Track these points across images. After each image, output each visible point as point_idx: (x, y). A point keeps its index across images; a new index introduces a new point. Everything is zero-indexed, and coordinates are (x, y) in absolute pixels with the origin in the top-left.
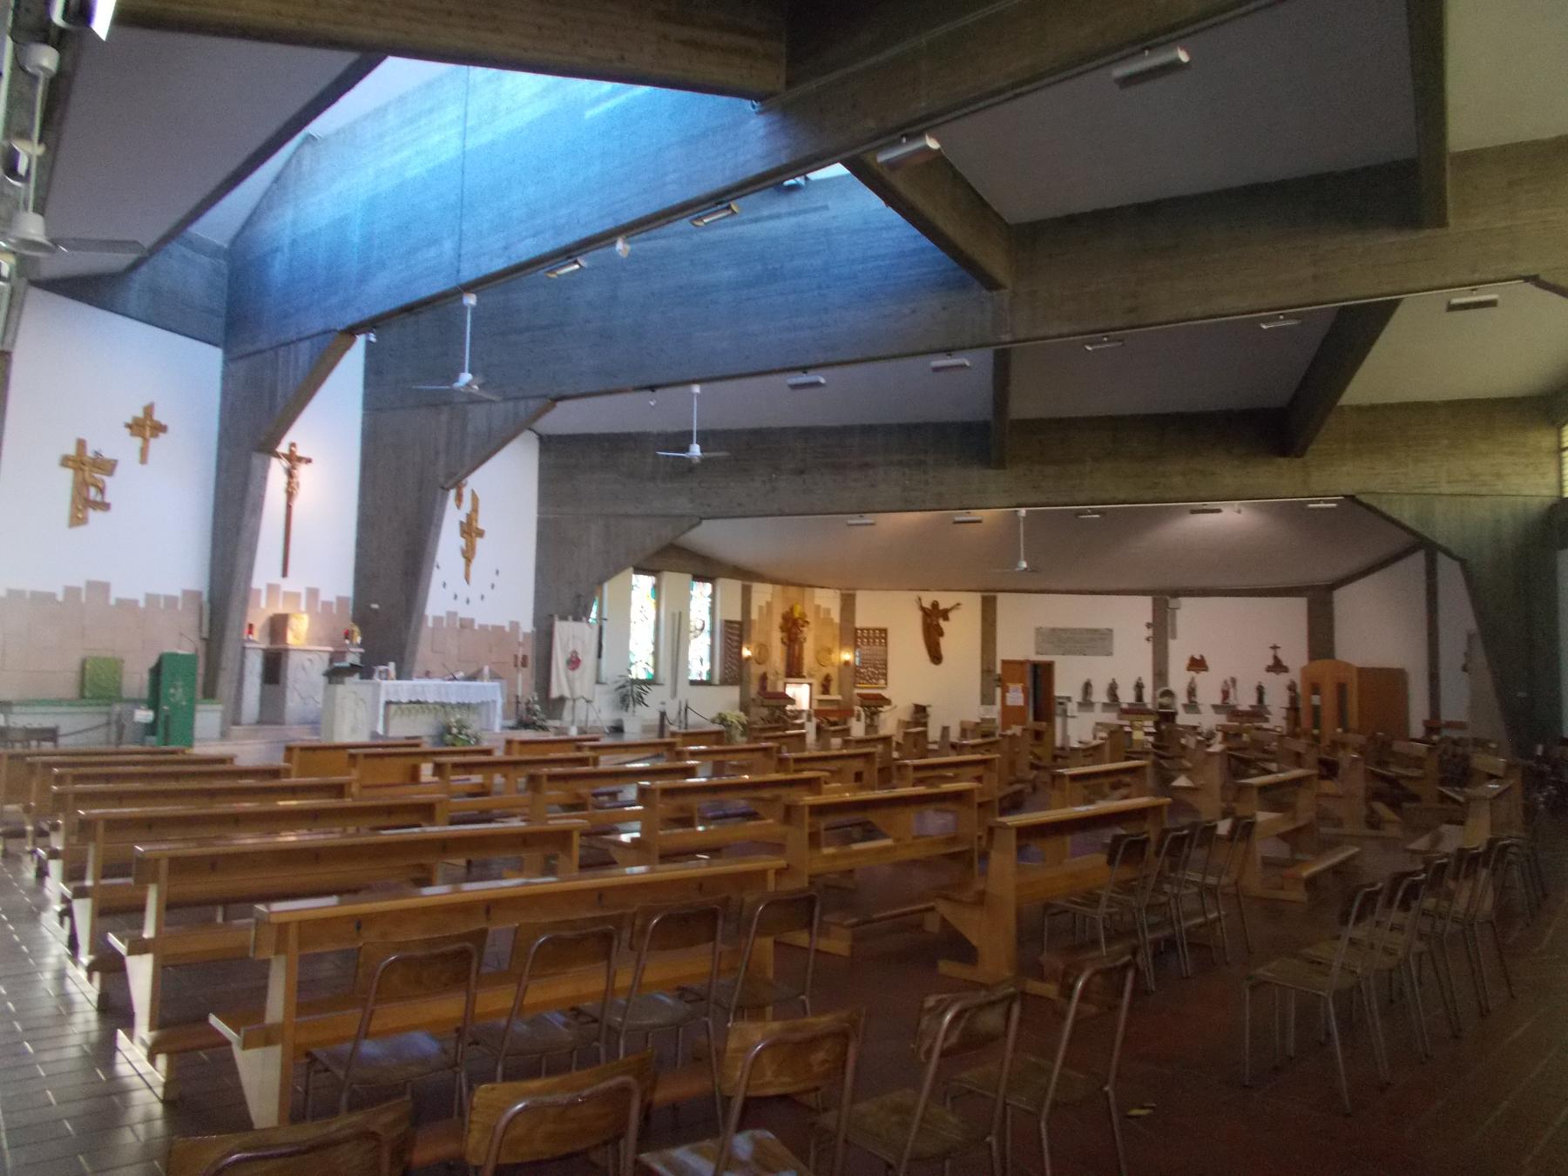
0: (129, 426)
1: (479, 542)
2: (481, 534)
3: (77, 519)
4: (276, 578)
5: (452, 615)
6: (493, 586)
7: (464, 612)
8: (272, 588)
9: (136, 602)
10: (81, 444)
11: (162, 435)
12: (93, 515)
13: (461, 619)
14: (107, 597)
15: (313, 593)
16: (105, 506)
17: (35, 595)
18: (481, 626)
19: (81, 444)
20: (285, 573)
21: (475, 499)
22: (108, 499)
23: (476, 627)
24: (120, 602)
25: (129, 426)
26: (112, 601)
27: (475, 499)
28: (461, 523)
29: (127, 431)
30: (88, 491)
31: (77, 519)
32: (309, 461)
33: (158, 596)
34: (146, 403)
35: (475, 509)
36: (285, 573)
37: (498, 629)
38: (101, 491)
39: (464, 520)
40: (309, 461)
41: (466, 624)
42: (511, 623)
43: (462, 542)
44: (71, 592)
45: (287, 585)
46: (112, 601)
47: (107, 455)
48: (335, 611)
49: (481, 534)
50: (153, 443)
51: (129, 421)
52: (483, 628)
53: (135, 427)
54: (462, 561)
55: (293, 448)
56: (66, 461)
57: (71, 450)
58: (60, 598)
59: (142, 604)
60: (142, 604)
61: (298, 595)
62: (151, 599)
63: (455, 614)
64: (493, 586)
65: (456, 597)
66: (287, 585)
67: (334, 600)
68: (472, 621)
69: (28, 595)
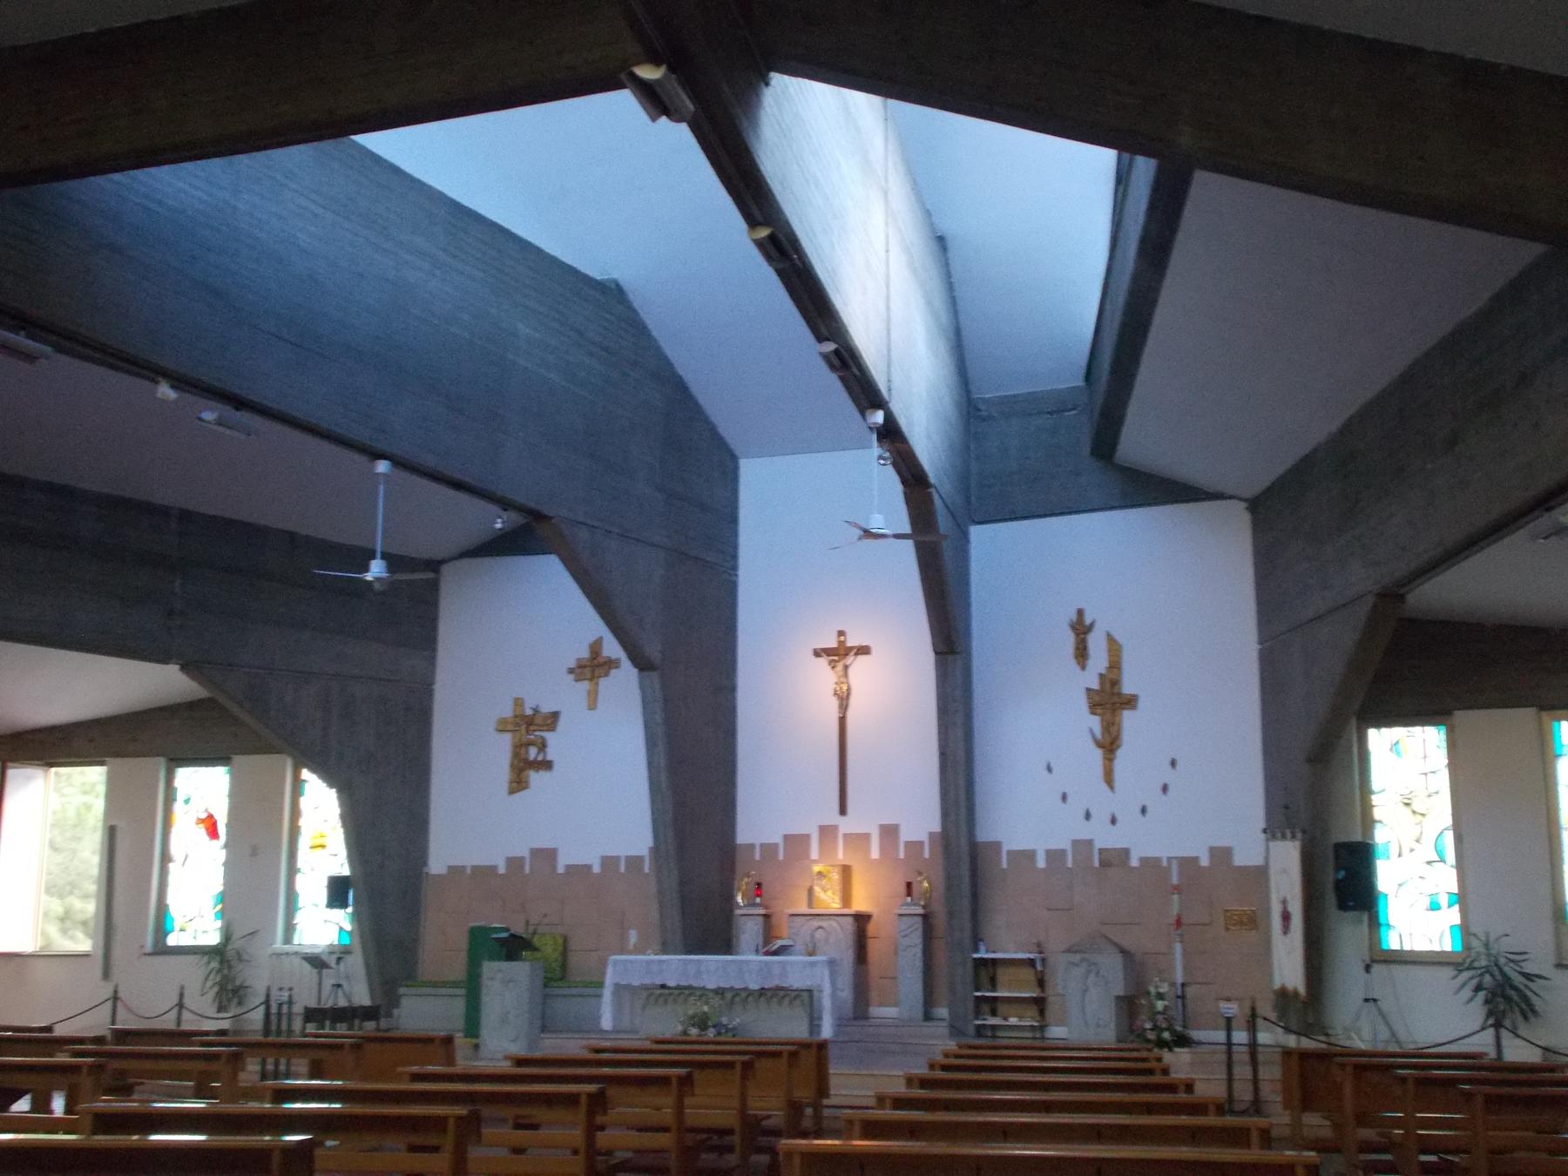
0: (571, 671)
1: (1128, 718)
2: (1131, 702)
3: (518, 783)
4: (832, 817)
5: (1083, 846)
6: (1165, 789)
7: (1105, 838)
8: (827, 832)
9: (589, 867)
10: (518, 702)
11: (613, 672)
12: (535, 778)
13: (1101, 851)
14: (554, 867)
15: (889, 833)
16: (547, 765)
17: (475, 868)
18: (1144, 860)
19: (518, 702)
20: (843, 810)
21: (1114, 648)
22: (549, 758)
23: (1134, 863)
24: (568, 867)
25: (571, 671)
26: (561, 870)
27: (1114, 648)
28: (1088, 690)
29: (571, 677)
30: (527, 753)
31: (518, 783)
32: (864, 650)
33: (617, 859)
34: (592, 639)
35: (1115, 665)
36: (843, 810)
37: (1188, 864)
38: (543, 746)
39: (1095, 685)
40: (864, 650)
41: (1114, 859)
42: (1213, 851)
43: (1095, 723)
44: (514, 863)
45: (846, 825)
46: (561, 870)
47: (546, 708)
48: (927, 854)
49: (1131, 702)
50: (603, 682)
51: (572, 664)
52: (1150, 863)
53: (578, 671)
54: (1098, 754)
55: (842, 638)
56: (502, 726)
57: (507, 711)
58: (502, 870)
59: (596, 869)
60: (596, 869)
61: (866, 837)
62: (609, 862)
63: (1090, 842)
64: (1165, 789)
65: (1088, 816)
66: (846, 825)
67: (924, 837)
68: (1126, 852)
69: (469, 871)
